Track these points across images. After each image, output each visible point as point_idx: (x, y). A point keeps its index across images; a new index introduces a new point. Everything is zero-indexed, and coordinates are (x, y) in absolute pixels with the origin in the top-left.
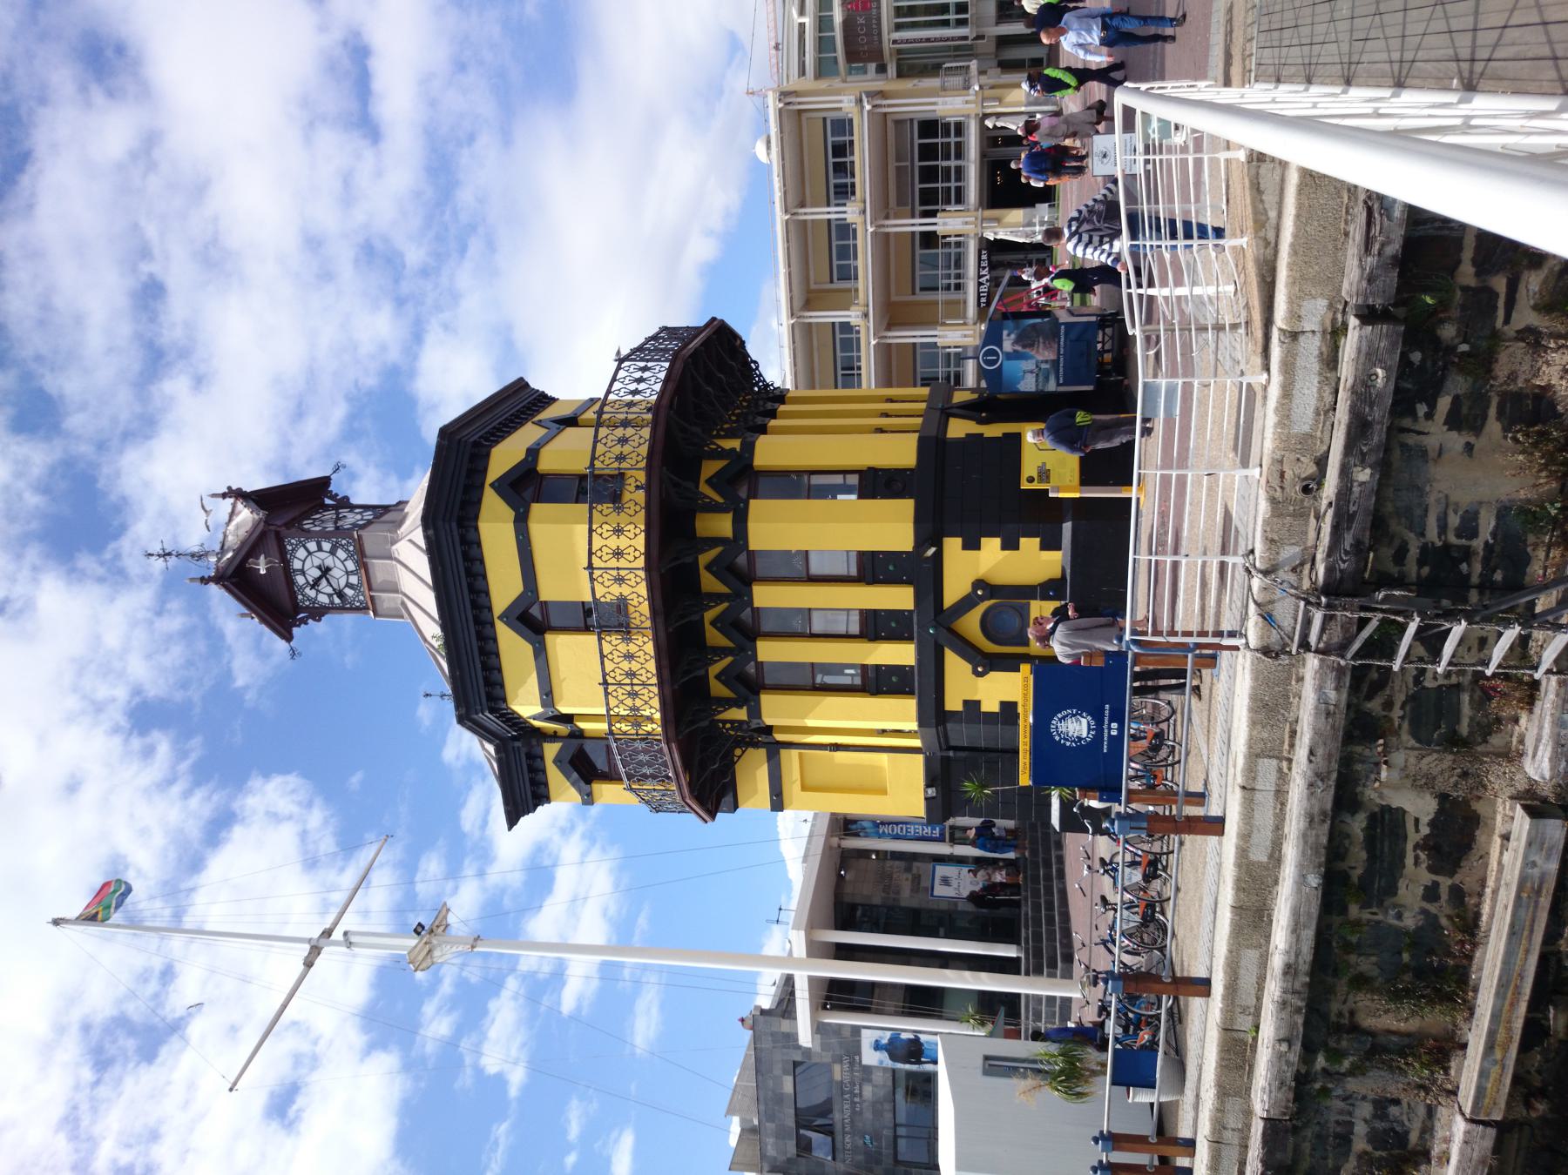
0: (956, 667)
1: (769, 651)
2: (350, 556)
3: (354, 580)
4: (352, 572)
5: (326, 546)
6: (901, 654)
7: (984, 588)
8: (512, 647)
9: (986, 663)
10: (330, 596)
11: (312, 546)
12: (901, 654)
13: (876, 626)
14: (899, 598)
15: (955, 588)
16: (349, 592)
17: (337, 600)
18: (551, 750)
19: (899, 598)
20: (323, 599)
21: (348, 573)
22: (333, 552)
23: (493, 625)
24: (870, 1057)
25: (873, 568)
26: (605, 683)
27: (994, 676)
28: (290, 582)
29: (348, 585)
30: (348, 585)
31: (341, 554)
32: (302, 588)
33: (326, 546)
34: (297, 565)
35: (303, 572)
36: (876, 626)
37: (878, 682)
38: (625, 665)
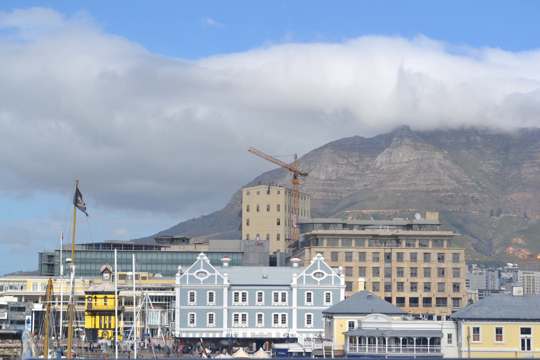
0: (102, 331)
1: (103, 317)
6: (103, 327)
7: (108, 333)
8: (103, 296)
9: (102, 333)
12: (103, 327)
13: (105, 325)
14: (107, 327)
15: (109, 331)
18: (91, 296)
19: (107, 327)
24: (27, 317)
25: (110, 325)
36: (105, 325)
37: (100, 325)
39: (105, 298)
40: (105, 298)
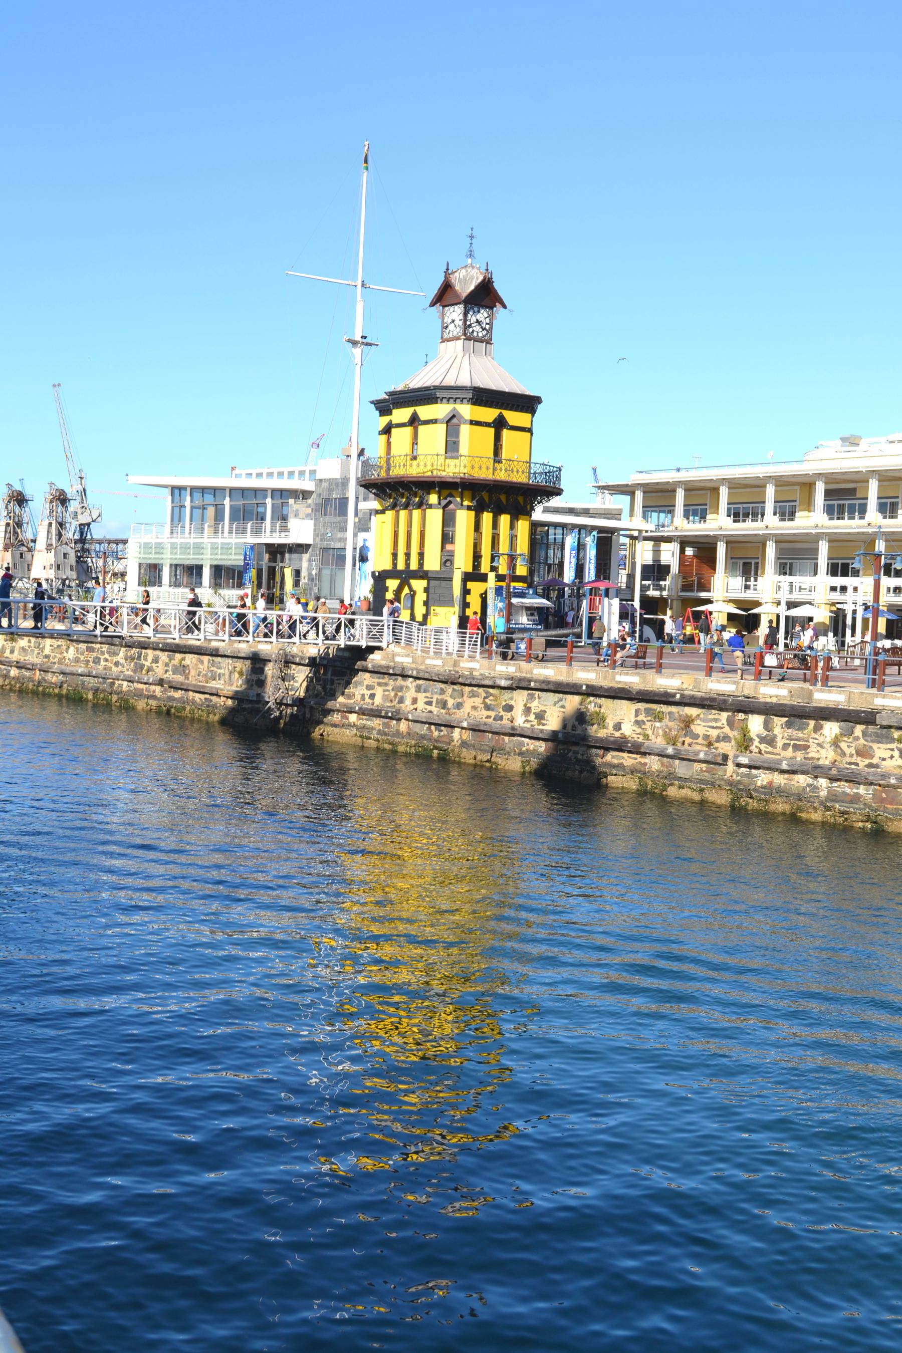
3: (475, 334)
8: (489, 414)
11: (488, 320)
16: (471, 330)
17: (468, 323)
23: (496, 407)
26: (510, 460)
27: (480, 600)
28: (476, 305)
29: (473, 331)
30: (473, 331)
33: (487, 327)
38: (515, 470)
39: (500, 424)
40: (500, 424)
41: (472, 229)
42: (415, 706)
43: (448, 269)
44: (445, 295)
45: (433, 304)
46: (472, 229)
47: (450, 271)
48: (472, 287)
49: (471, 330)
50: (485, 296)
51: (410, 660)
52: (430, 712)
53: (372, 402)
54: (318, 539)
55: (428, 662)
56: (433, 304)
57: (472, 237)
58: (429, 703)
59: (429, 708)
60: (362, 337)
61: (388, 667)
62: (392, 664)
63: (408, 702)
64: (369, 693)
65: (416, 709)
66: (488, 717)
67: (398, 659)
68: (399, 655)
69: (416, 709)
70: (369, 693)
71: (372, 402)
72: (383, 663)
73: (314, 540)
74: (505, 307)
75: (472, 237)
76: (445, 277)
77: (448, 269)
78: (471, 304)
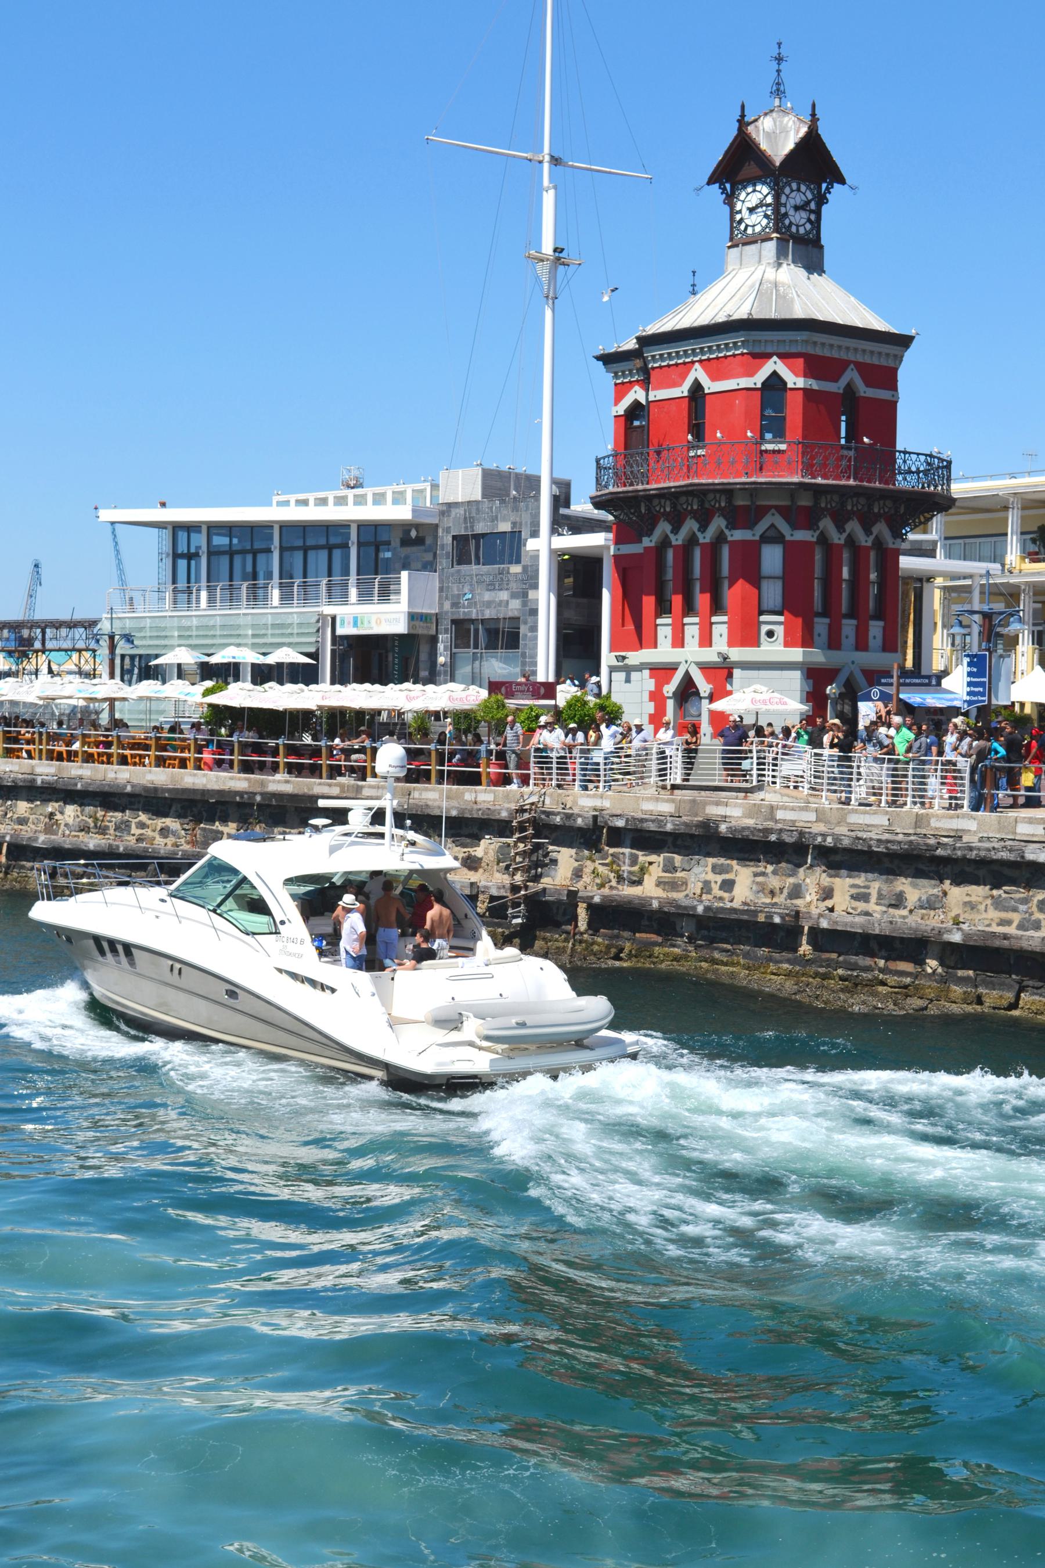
2: (807, 233)
3: (794, 229)
4: (798, 230)
5: (813, 217)
10: (785, 205)
16: (787, 222)
17: (783, 210)
20: (783, 199)
21: (798, 226)
22: (809, 220)
28: (794, 179)
31: (808, 226)
32: (790, 186)
33: (813, 217)
34: (803, 188)
35: (798, 190)
41: (779, 44)
42: (829, 903)
43: (743, 116)
44: (740, 163)
45: (710, 182)
46: (779, 44)
47: (746, 119)
48: (790, 146)
49: (787, 222)
50: (814, 163)
51: (812, 817)
52: (867, 914)
53: (598, 358)
54: (447, 606)
55: (853, 819)
56: (710, 182)
57: (779, 59)
58: (864, 897)
59: (861, 906)
60: (555, 250)
61: (767, 831)
62: (770, 824)
63: (811, 896)
64: (719, 878)
65: (831, 910)
66: (1003, 922)
67: (780, 815)
68: (785, 808)
69: (831, 910)
70: (719, 878)
71: (598, 358)
72: (750, 822)
73: (441, 605)
74: (842, 181)
75: (779, 59)
76: (740, 129)
77: (743, 116)
78: (787, 177)
